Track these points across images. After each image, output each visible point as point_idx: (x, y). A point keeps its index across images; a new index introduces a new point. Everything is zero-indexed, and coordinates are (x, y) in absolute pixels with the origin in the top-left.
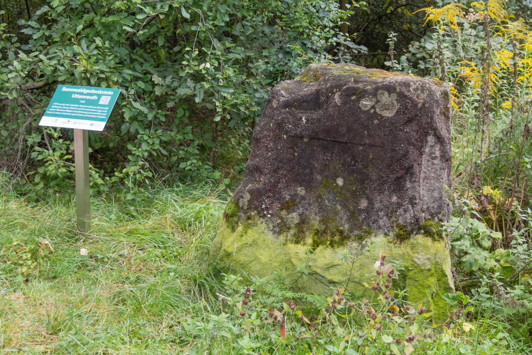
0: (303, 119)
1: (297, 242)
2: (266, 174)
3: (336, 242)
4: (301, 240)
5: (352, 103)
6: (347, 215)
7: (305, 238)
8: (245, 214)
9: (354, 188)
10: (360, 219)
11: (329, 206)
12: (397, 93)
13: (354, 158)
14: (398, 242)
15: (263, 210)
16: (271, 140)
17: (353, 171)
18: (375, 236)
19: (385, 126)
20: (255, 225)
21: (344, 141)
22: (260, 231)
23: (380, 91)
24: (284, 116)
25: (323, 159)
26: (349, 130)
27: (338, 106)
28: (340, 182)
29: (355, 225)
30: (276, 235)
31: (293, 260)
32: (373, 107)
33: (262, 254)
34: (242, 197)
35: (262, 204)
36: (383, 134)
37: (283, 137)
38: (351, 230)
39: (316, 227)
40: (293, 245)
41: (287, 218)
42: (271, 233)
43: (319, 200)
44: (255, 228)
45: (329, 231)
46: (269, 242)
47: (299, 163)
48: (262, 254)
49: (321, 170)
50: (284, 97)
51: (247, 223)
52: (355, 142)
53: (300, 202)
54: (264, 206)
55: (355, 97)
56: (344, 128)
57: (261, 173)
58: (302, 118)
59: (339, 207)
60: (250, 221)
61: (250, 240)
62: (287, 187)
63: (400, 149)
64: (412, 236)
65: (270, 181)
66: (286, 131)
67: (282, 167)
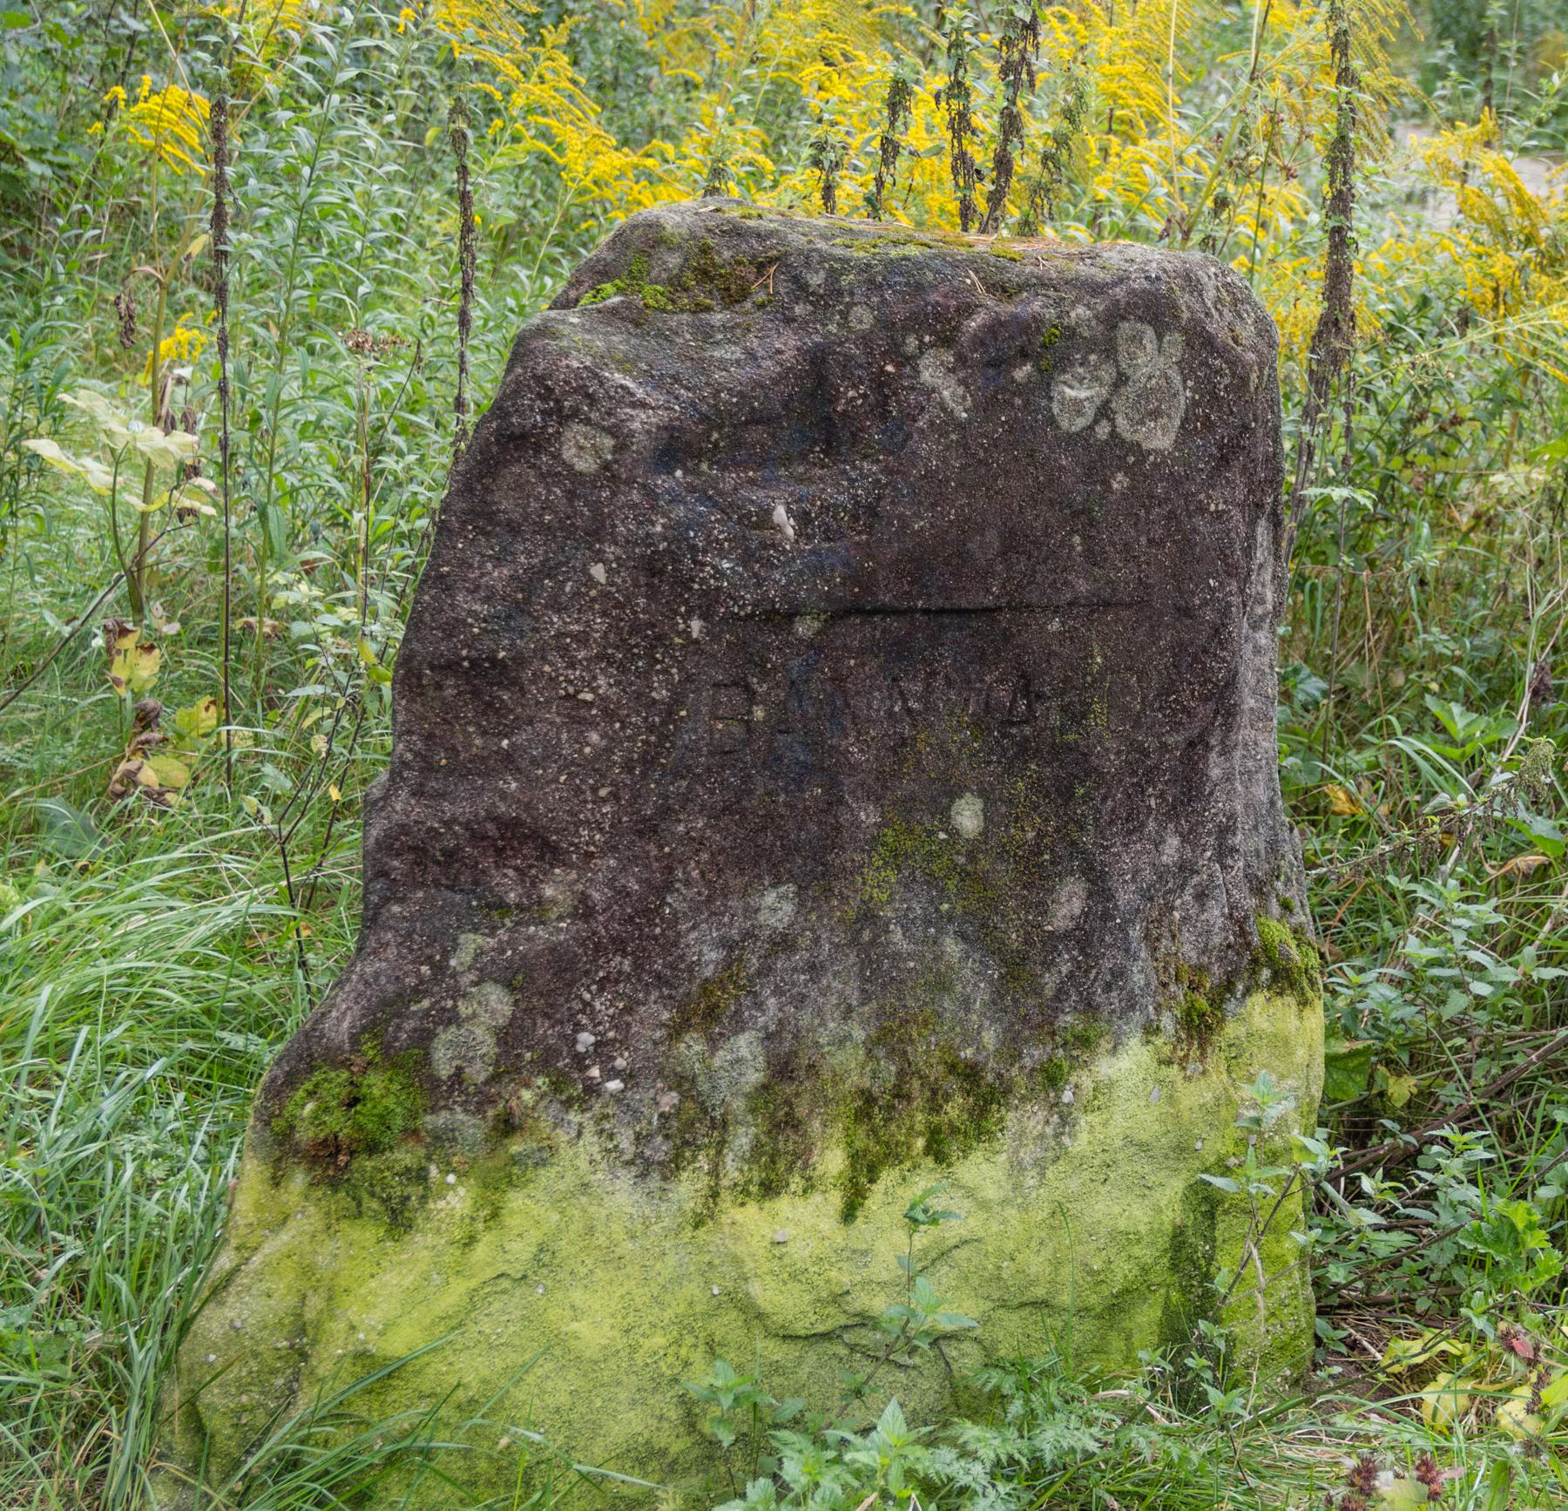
0: (780, 514)
1: (770, 1189)
2: (589, 856)
3: (954, 1130)
4: (790, 1170)
5: (1018, 401)
6: (991, 981)
7: (809, 1150)
8: (480, 1110)
9: (1031, 835)
10: (1050, 981)
11: (910, 956)
12: (1184, 331)
13: (1027, 687)
14: (1195, 1052)
15: (580, 1062)
16: (600, 657)
17: (1024, 750)
18: (1114, 1051)
19: (1151, 496)
20: (545, 1156)
21: (989, 601)
22: (570, 1180)
23: (1125, 327)
24: (680, 512)
25: (890, 714)
26: (1012, 543)
27: (961, 426)
28: (968, 817)
29: (1025, 1019)
30: (655, 1182)
31: (755, 1288)
32: (1104, 411)
33: (576, 1313)
34: (452, 1018)
35: (578, 1028)
36: (1143, 540)
37: (686, 633)
38: (1012, 1049)
39: (855, 1080)
40: (752, 1208)
41: (711, 1075)
42: (626, 1177)
43: (866, 936)
44: (546, 1175)
45: (916, 1084)
46: (617, 1229)
47: (772, 760)
48: (576, 1313)
49: (881, 776)
50: (643, 405)
51: (499, 1161)
52: (1034, 598)
53: (765, 971)
54: (586, 1039)
55: (1028, 368)
56: (992, 536)
57: (551, 853)
58: (768, 512)
59: (952, 947)
60: (516, 1147)
61: (521, 1251)
62: (710, 904)
63: (1205, 603)
64: (1230, 1006)
65: (624, 893)
66: (705, 593)
67: (686, 799)
